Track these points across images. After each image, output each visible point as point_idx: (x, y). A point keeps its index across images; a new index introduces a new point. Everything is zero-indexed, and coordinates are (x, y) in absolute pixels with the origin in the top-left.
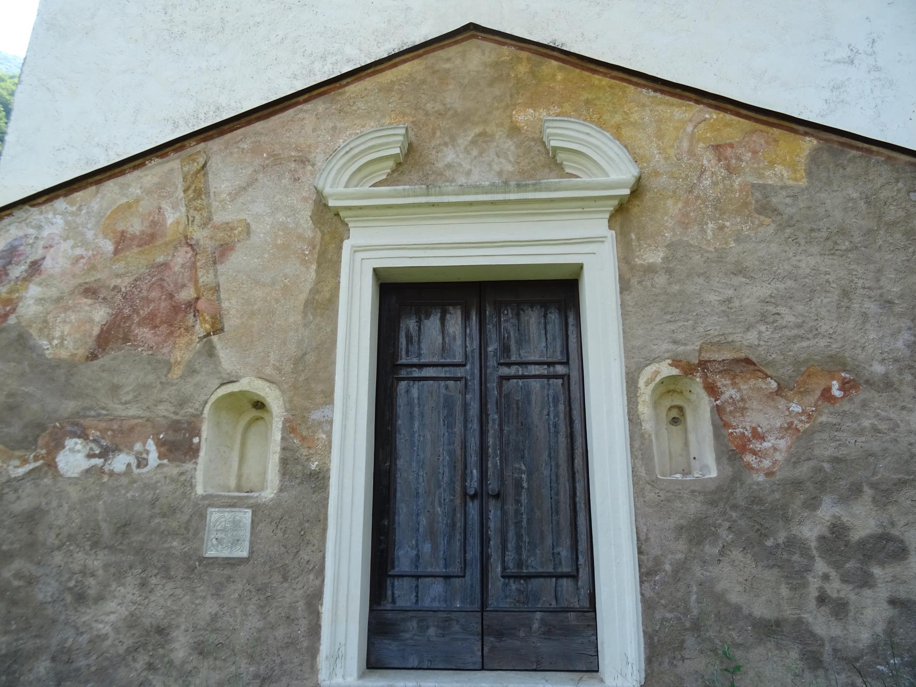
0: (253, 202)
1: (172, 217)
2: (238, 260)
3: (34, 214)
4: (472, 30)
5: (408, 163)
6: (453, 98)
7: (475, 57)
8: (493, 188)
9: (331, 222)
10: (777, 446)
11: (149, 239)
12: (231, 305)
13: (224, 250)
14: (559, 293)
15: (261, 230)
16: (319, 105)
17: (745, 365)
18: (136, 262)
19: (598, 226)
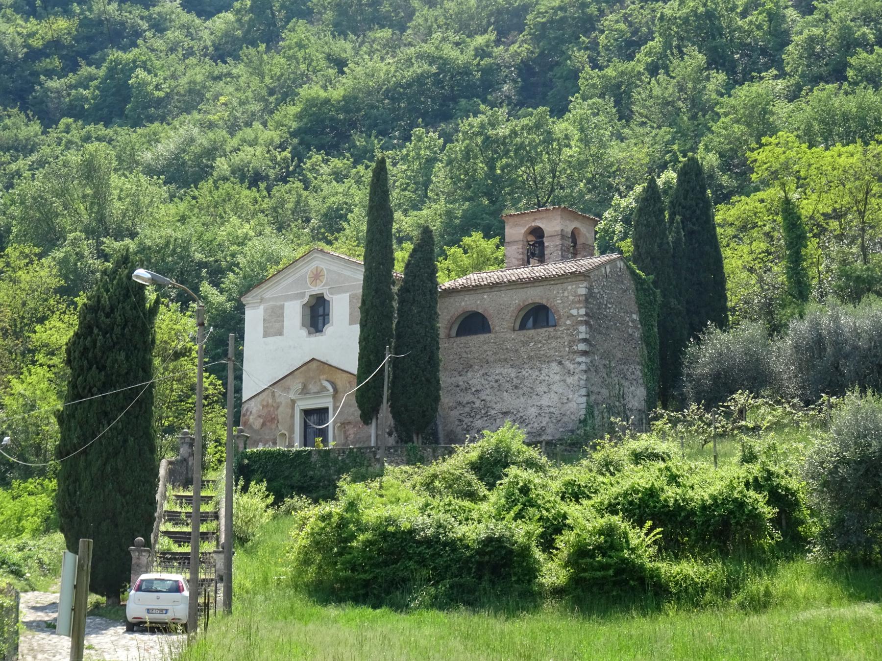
0: (283, 397)
1: (270, 401)
2: (281, 409)
3: (250, 402)
4: (313, 359)
5: (305, 391)
6: (311, 374)
7: (314, 365)
8: (315, 393)
9: (293, 402)
10: (352, 436)
11: (267, 406)
12: (280, 417)
13: (278, 407)
14: (326, 410)
15: (283, 403)
16: (290, 377)
17: (349, 423)
18: (266, 411)
19: (331, 399)
